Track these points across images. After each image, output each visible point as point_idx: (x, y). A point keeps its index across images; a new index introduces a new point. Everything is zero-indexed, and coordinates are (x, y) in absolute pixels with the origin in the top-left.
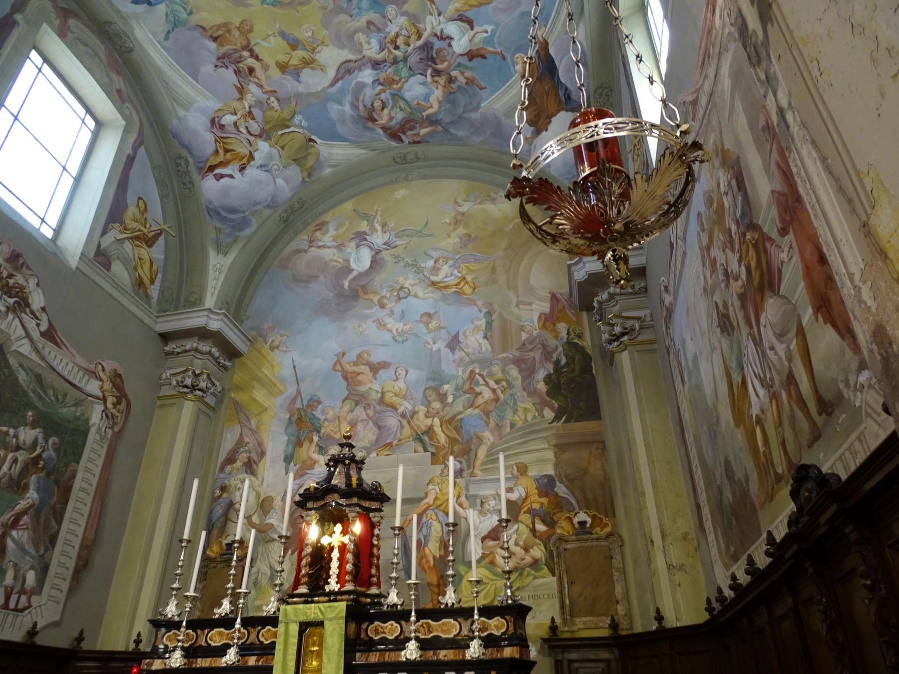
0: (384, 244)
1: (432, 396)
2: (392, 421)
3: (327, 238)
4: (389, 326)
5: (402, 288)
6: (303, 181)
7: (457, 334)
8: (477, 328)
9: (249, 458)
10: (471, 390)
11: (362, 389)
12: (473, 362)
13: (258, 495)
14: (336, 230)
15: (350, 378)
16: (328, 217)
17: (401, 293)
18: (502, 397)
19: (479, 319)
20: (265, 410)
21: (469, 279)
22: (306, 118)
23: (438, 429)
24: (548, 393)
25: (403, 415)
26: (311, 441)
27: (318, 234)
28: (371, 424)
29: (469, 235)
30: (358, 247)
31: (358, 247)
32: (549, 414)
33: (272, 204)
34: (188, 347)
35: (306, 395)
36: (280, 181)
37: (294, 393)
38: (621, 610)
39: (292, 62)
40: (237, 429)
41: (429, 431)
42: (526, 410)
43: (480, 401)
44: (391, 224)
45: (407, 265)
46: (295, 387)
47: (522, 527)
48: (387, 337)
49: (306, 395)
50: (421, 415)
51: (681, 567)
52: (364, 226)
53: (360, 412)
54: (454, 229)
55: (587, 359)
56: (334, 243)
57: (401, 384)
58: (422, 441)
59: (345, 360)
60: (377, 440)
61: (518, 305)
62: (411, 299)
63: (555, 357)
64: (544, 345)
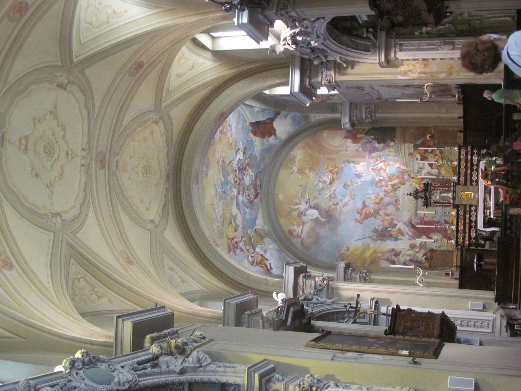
0: (306, 204)
1: (380, 184)
2: (387, 199)
3: (297, 229)
4: (347, 201)
5: (330, 196)
6: (270, 238)
7: (355, 174)
8: (354, 167)
9: (394, 255)
10: (379, 170)
11: (372, 211)
12: (368, 169)
13: (409, 250)
14: (294, 225)
15: (367, 216)
16: (286, 229)
17: (333, 196)
18: (383, 159)
19: (350, 166)
20: (375, 251)
21: (331, 169)
22: (249, 229)
23: (393, 183)
24: (384, 143)
25: (385, 195)
26: (391, 231)
27: (294, 234)
28: (387, 208)
29: (310, 168)
30: (305, 215)
31: (305, 215)
32: (392, 144)
33: (280, 251)
34: (349, 277)
35: (371, 234)
36: (270, 247)
37: (370, 239)
38: (456, 129)
39: (234, 225)
40: (382, 261)
41: (393, 186)
42: (389, 151)
43: (384, 167)
44: (297, 201)
45: (319, 194)
46: (367, 239)
47: (430, 156)
48: (352, 202)
49: (371, 234)
50: (386, 189)
51: (447, 110)
52: (295, 213)
53: (382, 212)
54: (306, 174)
55: (373, 129)
56: (301, 227)
57: (373, 196)
58: (396, 188)
59: (359, 219)
60: (394, 205)
61: (346, 151)
62: (336, 192)
63: (370, 140)
64: (365, 143)
